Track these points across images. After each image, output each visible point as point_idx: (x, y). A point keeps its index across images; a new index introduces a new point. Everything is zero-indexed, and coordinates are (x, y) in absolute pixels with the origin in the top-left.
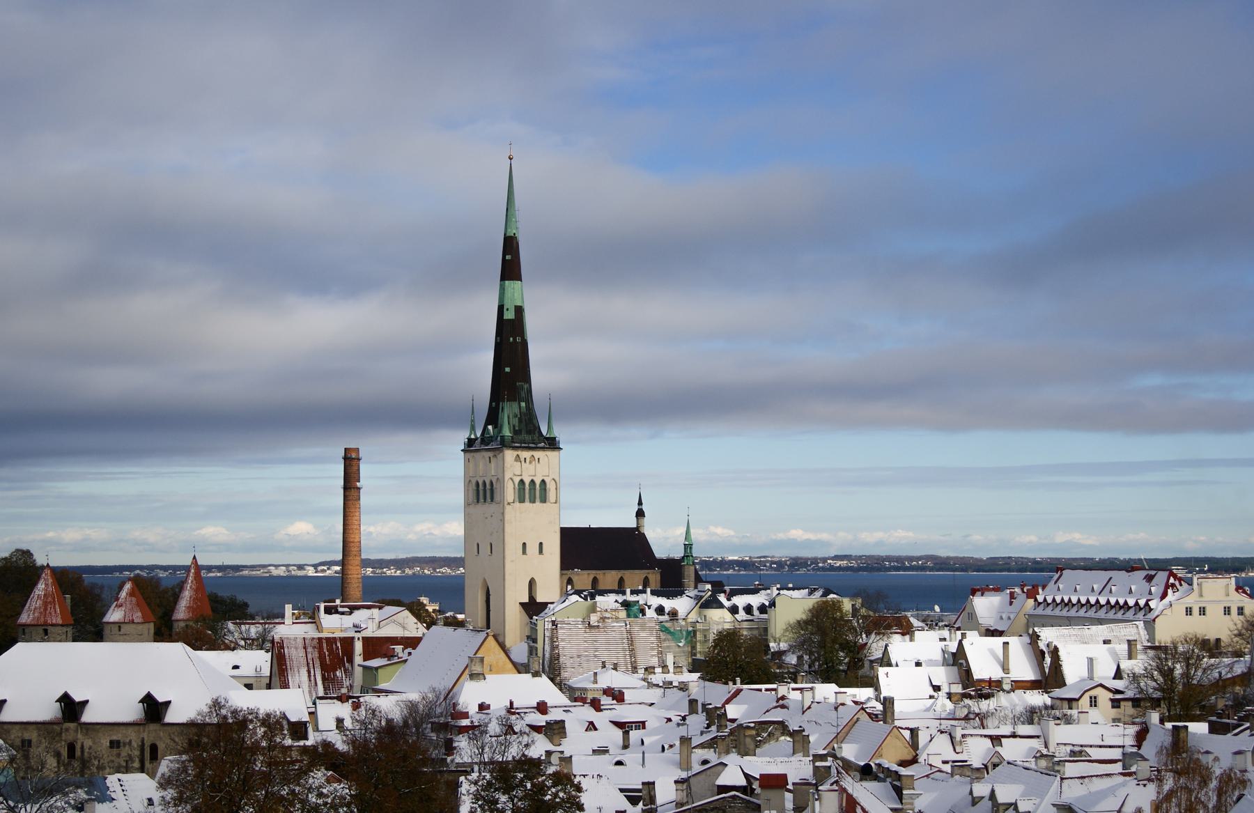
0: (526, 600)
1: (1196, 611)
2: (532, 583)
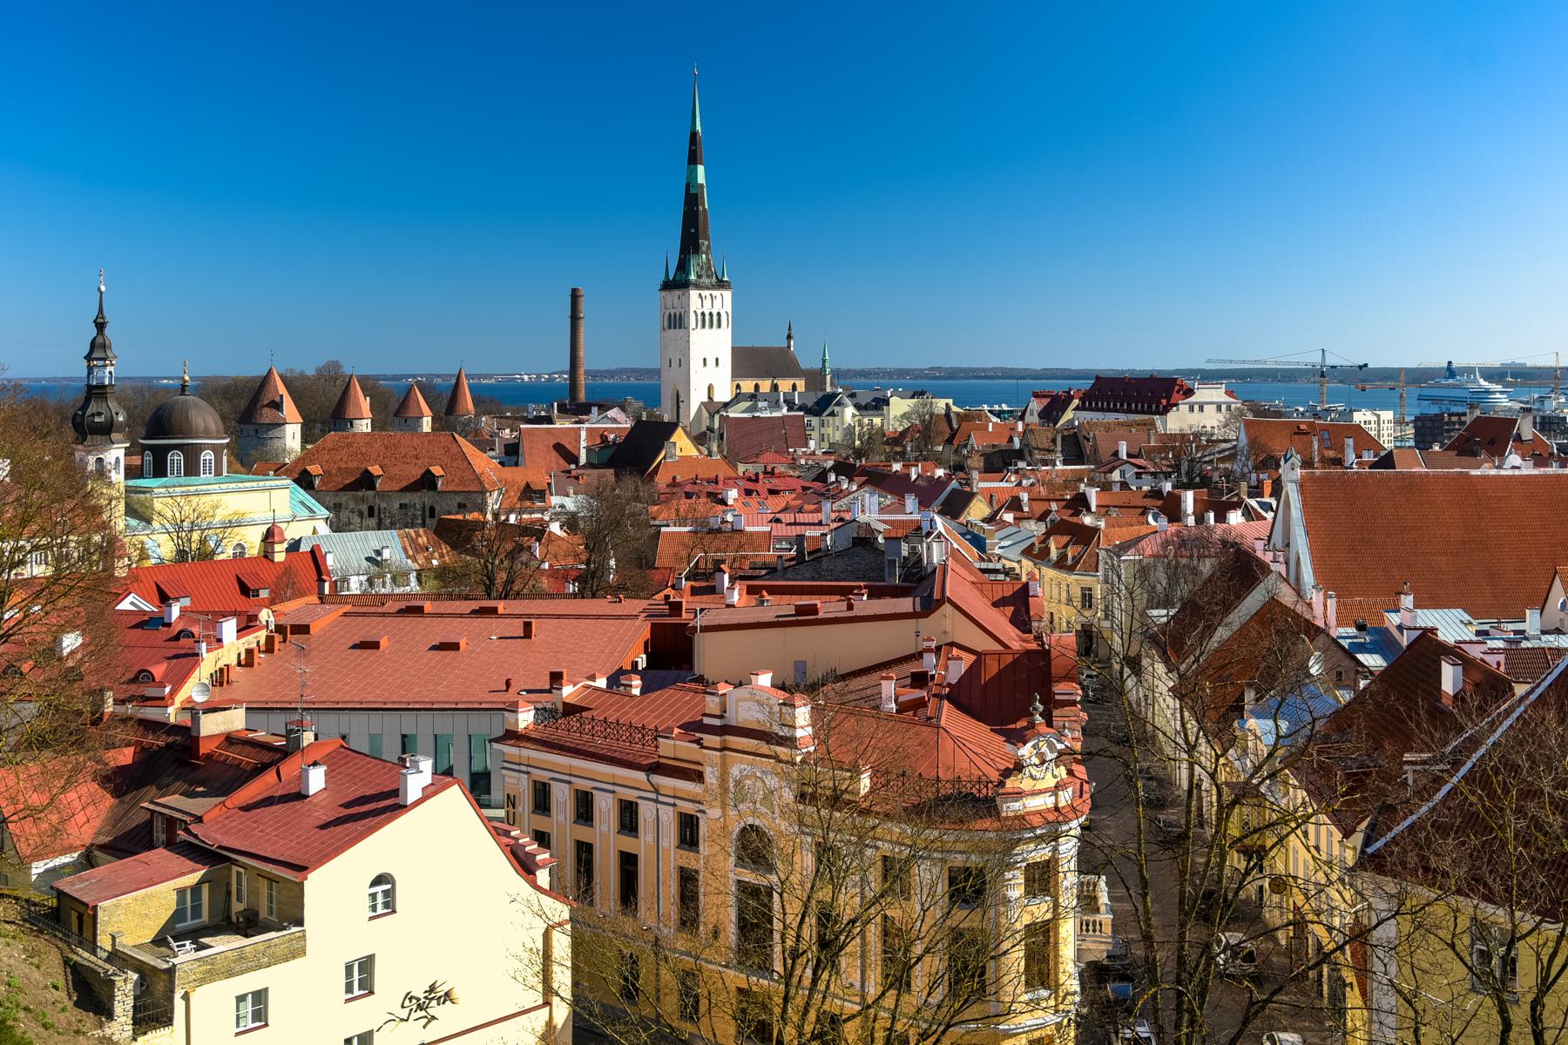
0: (706, 400)
1: (1196, 407)
2: (710, 388)
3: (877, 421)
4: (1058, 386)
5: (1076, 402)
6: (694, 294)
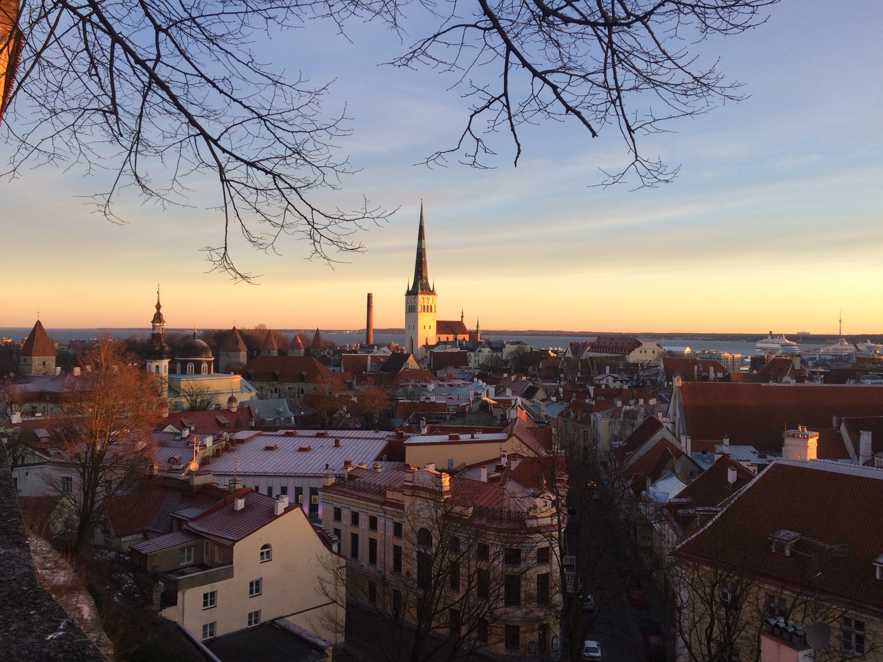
0: (425, 344)
1: (643, 352)
3: (499, 354)
4: (581, 340)
5: (589, 348)
6: (420, 297)
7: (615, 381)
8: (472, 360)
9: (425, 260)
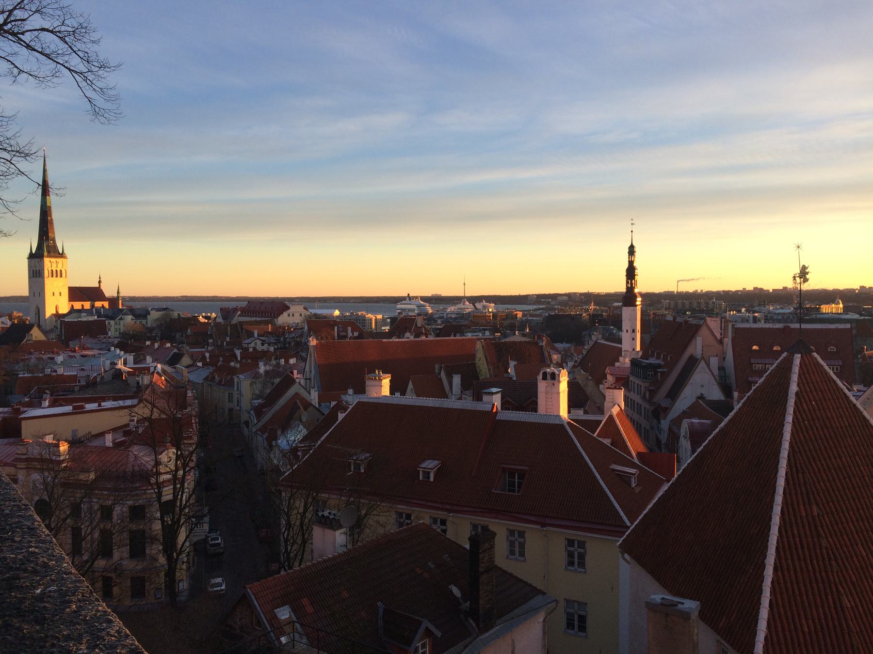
1: (291, 315)
2: (57, 307)
3: (144, 322)
4: (233, 305)
5: (239, 312)
6: (47, 260)
7: (263, 344)
8: (112, 329)
9: (52, 219)
